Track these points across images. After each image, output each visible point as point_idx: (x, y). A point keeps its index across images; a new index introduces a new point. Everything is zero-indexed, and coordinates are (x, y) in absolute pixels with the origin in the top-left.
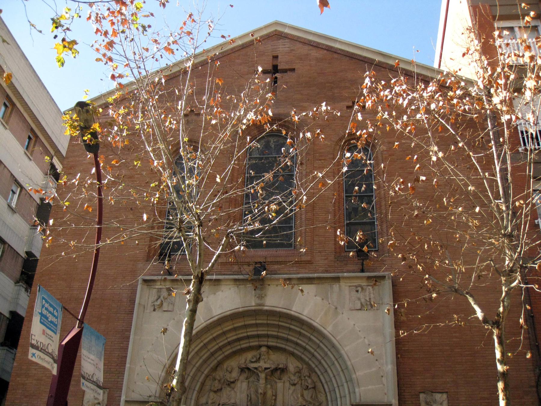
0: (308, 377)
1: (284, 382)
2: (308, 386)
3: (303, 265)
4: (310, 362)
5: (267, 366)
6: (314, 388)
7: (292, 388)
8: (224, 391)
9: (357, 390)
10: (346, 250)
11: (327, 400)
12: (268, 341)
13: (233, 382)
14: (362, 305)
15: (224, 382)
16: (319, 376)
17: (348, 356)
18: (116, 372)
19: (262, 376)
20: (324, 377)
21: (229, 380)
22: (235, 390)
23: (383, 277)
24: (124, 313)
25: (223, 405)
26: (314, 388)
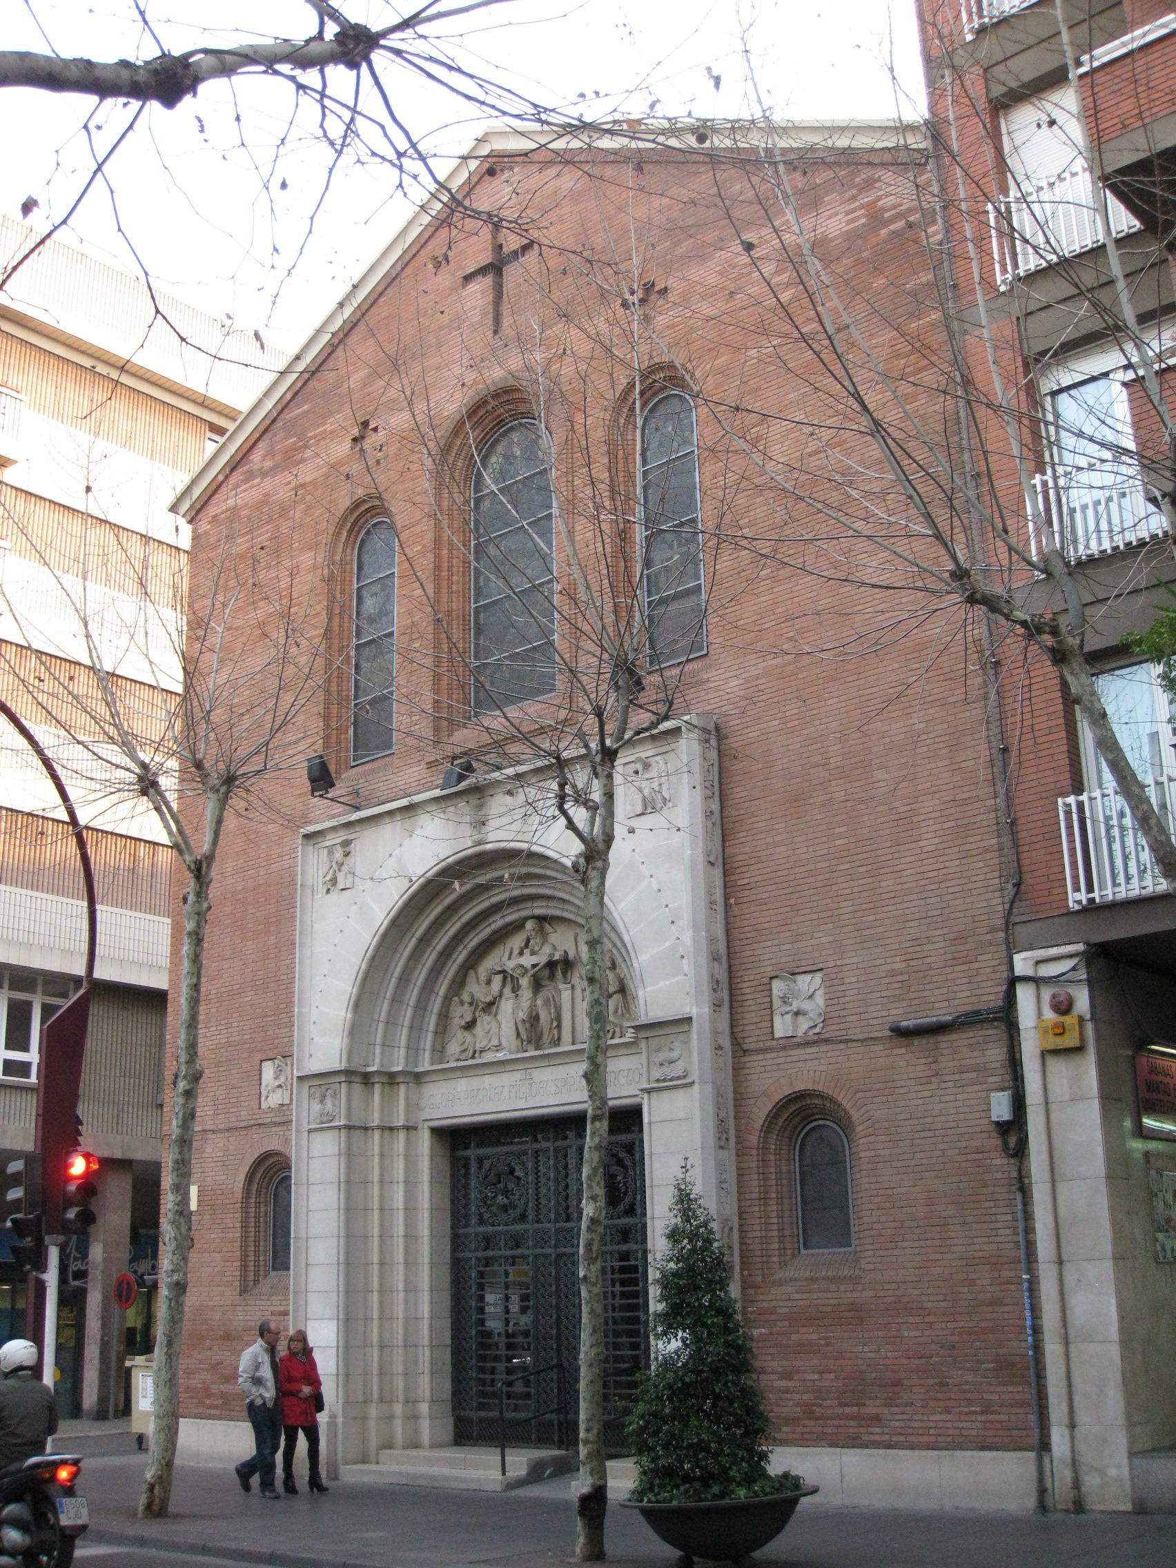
1: (573, 987)
13: (491, 1004)
19: (525, 982)
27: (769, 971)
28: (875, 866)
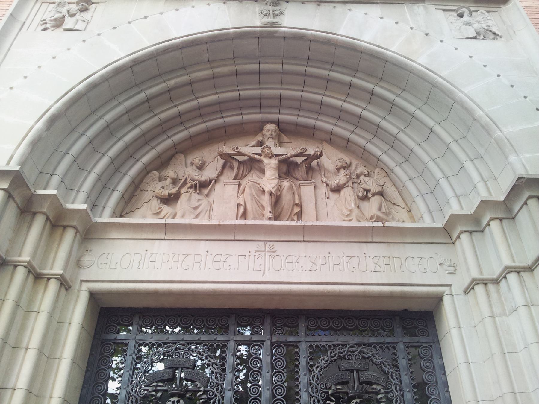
0: (365, 175)
6: (381, 194)
8: (184, 198)
17: (472, 100)
20: (403, 170)
22: (211, 199)
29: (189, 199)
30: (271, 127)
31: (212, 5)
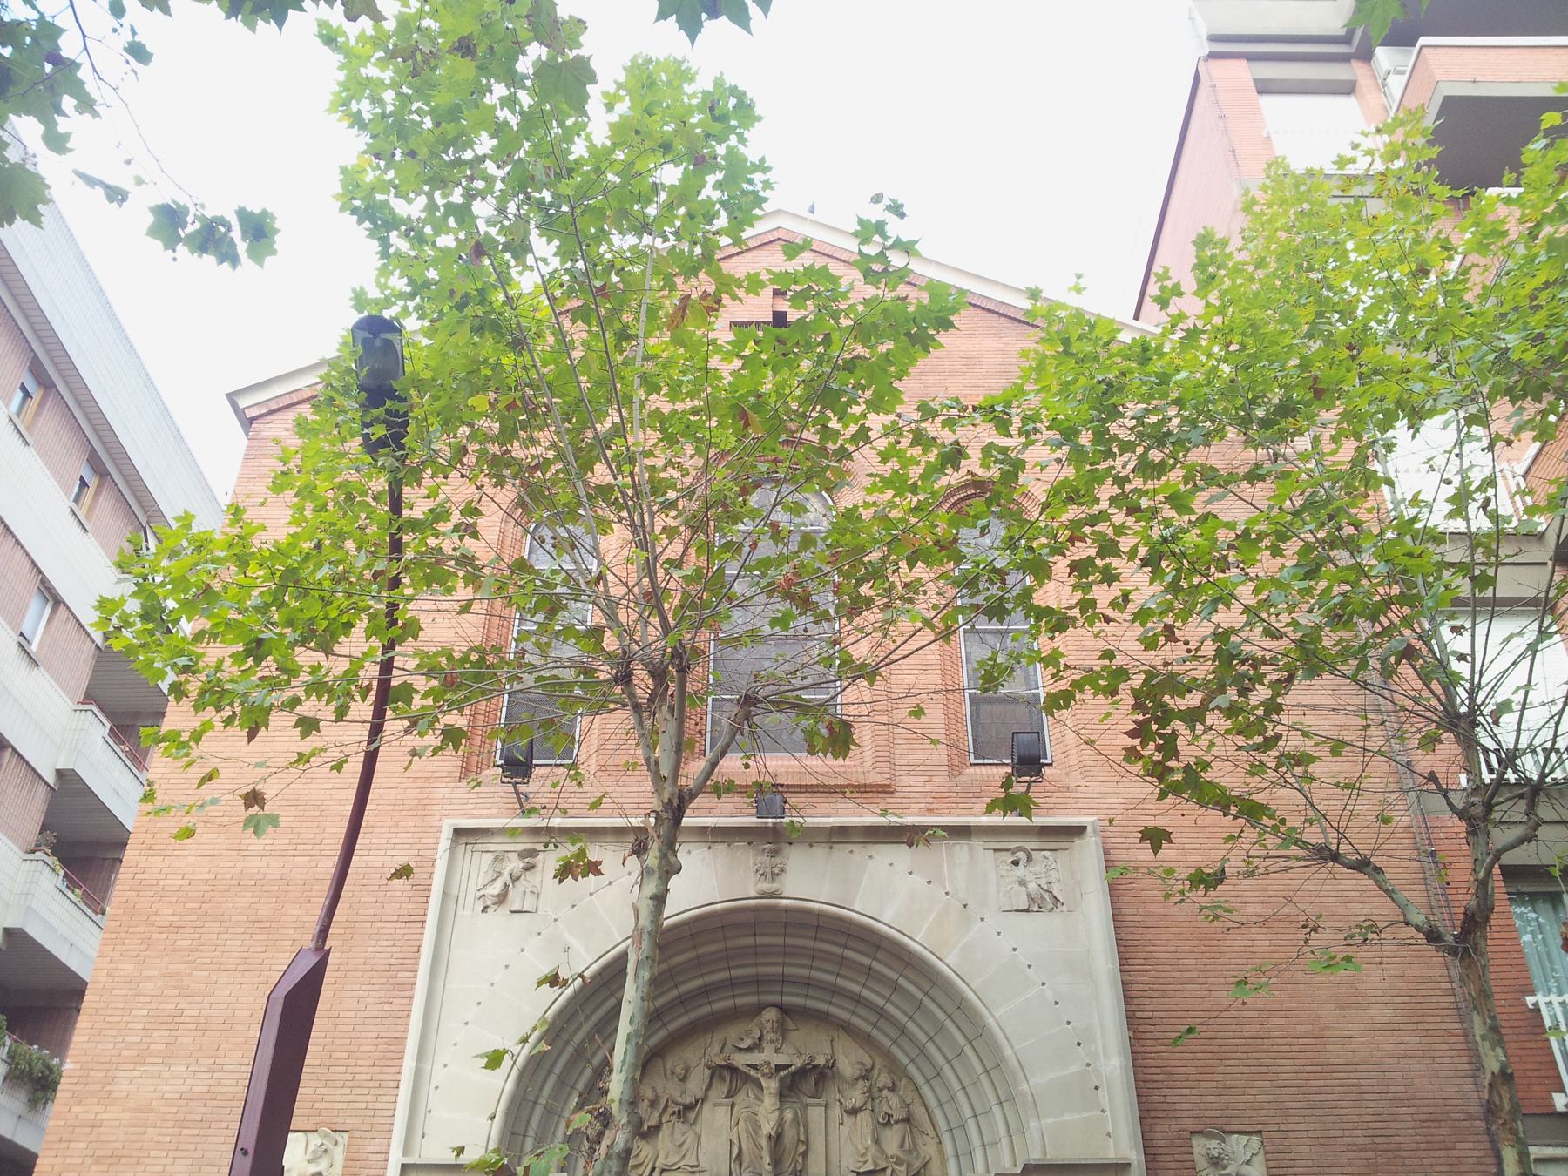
1: (827, 1106)
2: (890, 1116)
3: (870, 795)
4: (895, 1049)
5: (782, 1059)
6: (907, 1120)
7: (848, 1120)
9: (1033, 1124)
10: (973, 761)
11: (941, 1152)
12: (782, 993)
13: (689, 1108)
14: (1031, 899)
15: (666, 1107)
16: (917, 1089)
18: (371, 1084)
19: (771, 1085)
21: (679, 1100)
22: (698, 1128)
23: (1080, 830)
24: (396, 918)
25: (663, 1171)
26: (907, 1120)
27: (1189, 1123)
28: (1316, 1028)
29: (673, 1133)
30: (770, 1015)
31: (694, 853)
